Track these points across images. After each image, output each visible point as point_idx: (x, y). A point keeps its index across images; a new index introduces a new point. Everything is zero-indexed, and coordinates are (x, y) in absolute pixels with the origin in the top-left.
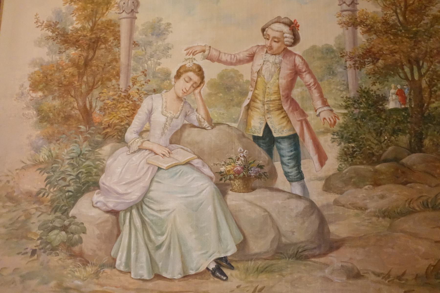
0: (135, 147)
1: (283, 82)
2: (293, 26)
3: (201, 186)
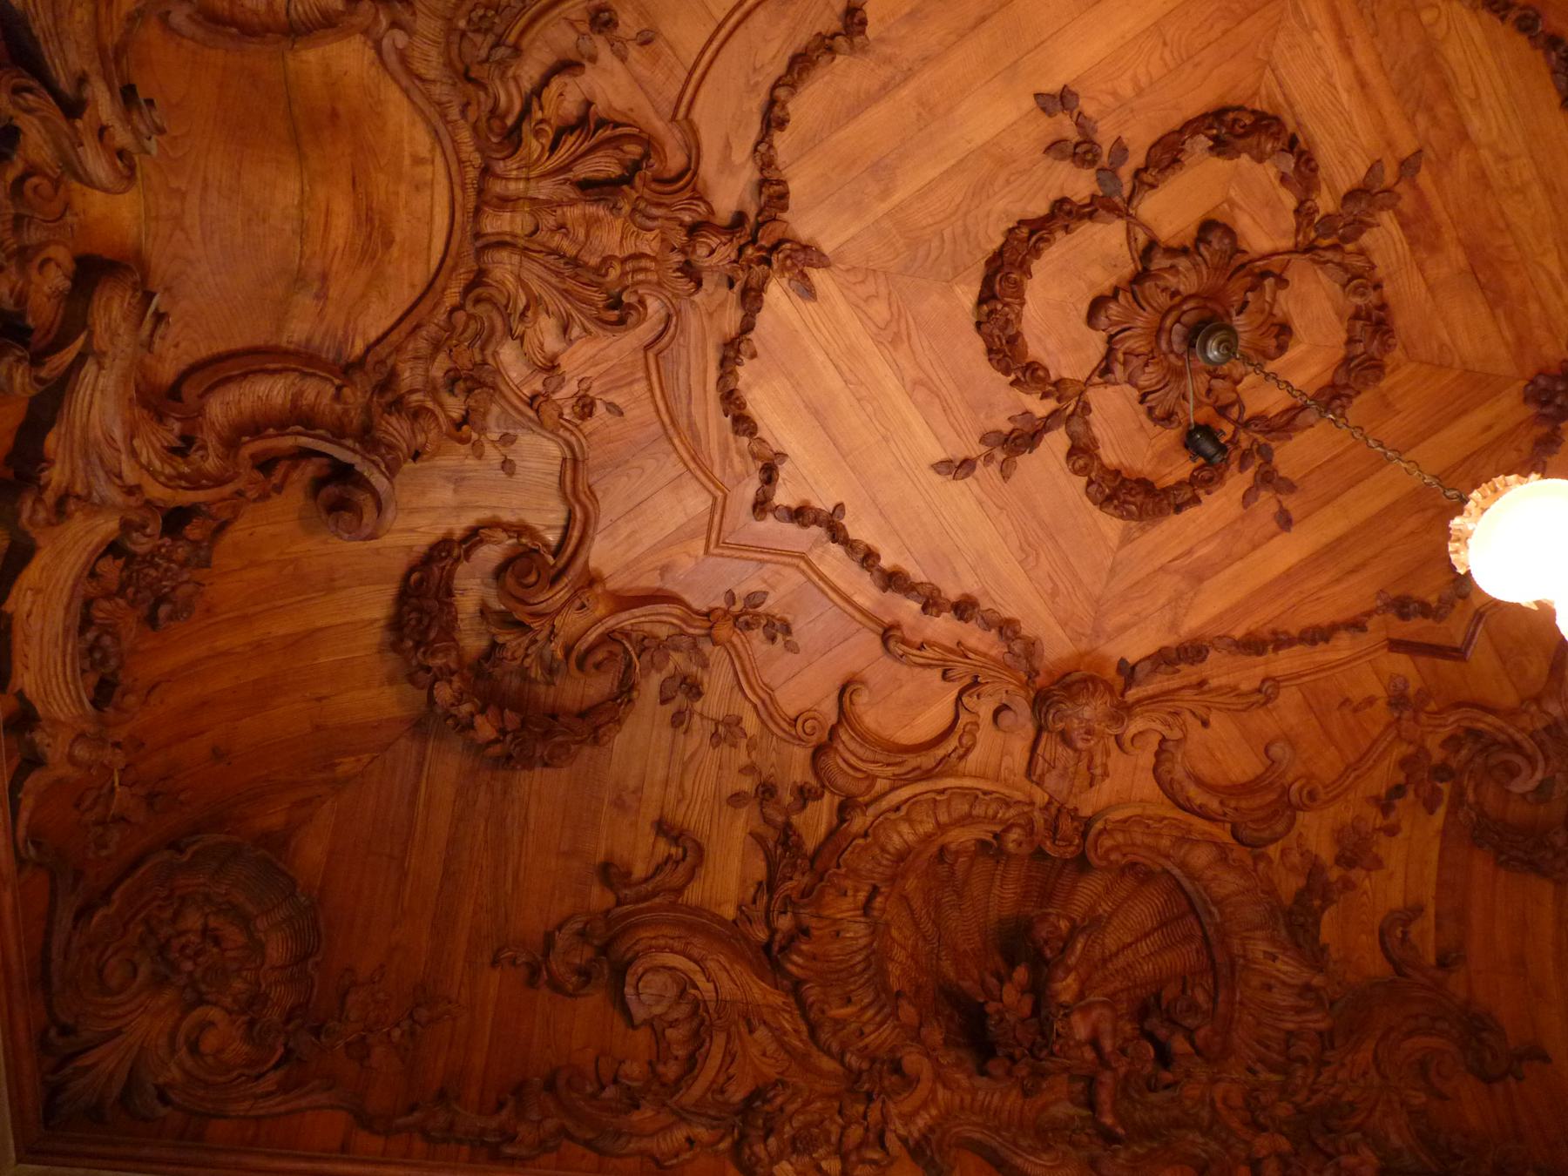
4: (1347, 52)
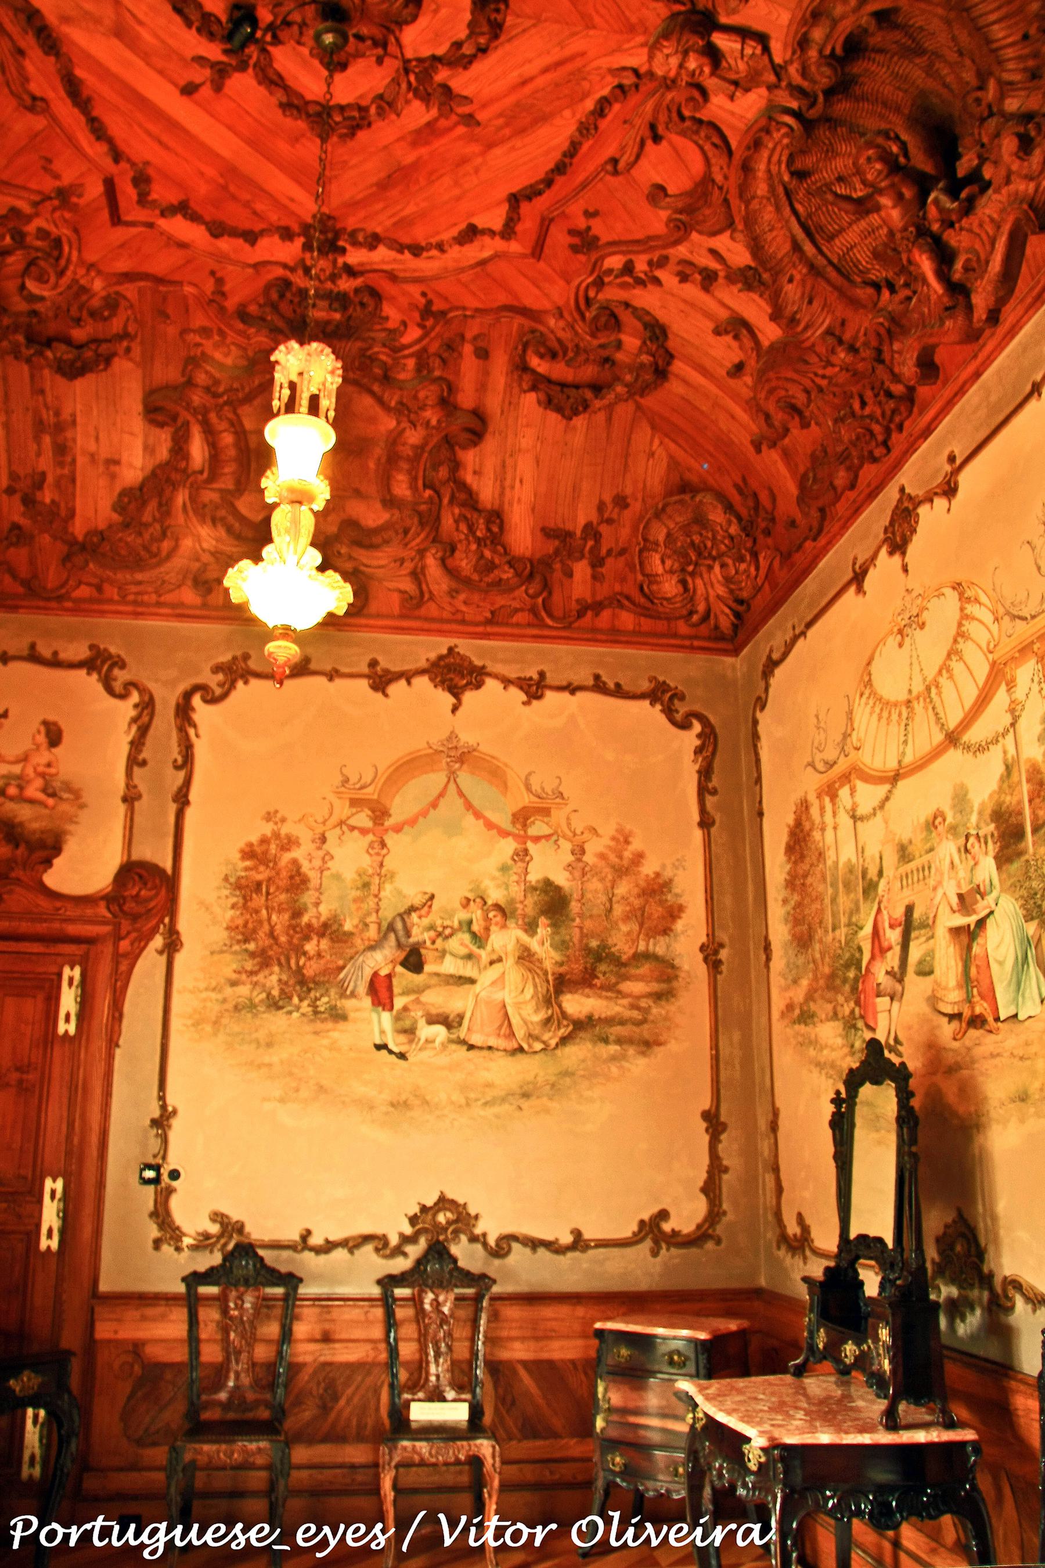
4: (546, 70)
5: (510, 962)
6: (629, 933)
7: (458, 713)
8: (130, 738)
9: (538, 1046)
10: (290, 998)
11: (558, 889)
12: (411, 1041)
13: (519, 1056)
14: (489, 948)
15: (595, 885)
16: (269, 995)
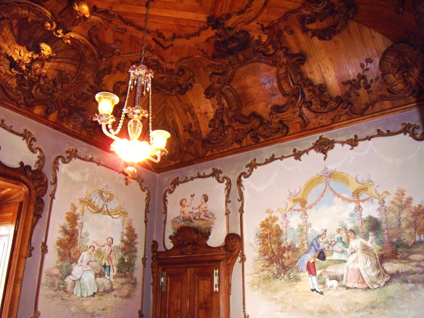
0: (80, 265)
1: (109, 253)
2: (112, 239)
3: (93, 276)
5: (359, 252)
6: (410, 234)
7: (326, 160)
8: (225, 195)
9: (376, 286)
10: (281, 274)
11: (375, 219)
12: (324, 287)
13: (368, 290)
14: (350, 247)
15: (391, 215)
16: (274, 273)
